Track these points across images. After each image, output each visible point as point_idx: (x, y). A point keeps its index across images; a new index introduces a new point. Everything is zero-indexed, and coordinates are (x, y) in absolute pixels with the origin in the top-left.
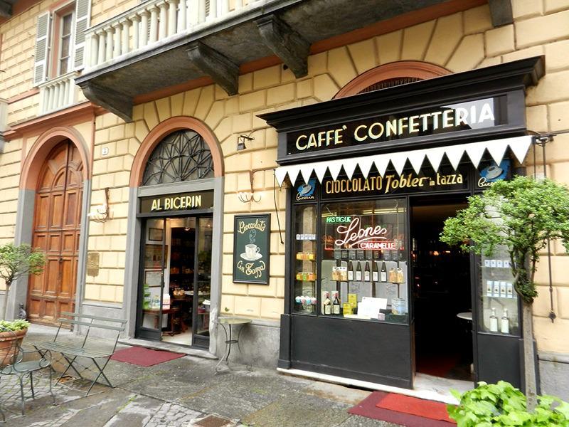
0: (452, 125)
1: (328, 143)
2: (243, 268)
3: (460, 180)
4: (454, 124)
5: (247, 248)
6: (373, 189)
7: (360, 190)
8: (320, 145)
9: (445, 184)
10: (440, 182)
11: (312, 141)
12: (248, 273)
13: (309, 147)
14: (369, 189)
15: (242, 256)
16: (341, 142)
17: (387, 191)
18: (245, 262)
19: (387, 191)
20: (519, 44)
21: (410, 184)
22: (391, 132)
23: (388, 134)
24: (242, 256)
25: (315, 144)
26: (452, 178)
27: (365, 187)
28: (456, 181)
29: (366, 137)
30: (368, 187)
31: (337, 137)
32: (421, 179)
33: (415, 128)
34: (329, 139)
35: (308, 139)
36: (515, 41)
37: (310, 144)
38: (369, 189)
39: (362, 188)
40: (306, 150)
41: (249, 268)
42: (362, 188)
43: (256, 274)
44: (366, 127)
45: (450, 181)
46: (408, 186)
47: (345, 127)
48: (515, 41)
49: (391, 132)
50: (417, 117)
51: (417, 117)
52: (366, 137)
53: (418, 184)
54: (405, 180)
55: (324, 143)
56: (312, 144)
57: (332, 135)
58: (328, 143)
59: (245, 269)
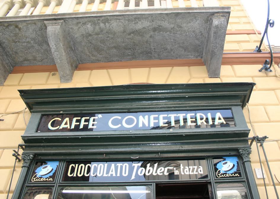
1: (81, 127)
3: (200, 171)
6: (118, 175)
7: (105, 175)
9: (188, 173)
10: (184, 172)
11: (66, 124)
13: (61, 128)
14: (114, 175)
17: (133, 177)
21: (156, 172)
22: (143, 124)
23: (140, 125)
26: (193, 169)
27: (110, 173)
28: (197, 171)
29: (120, 125)
32: (166, 169)
34: (83, 123)
37: (63, 126)
38: (114, 175)
39: (108, 173)
40: (55, 131)
42: (108, 173)
45: (193, 171)
46: (154, 174)
49: (143, 124)
50: (166, 115)
51: (166, 115)
52: (120, 125)
53: (163, 172)
54: (151, 168)
56: (66, 126)
58: (81, 127)
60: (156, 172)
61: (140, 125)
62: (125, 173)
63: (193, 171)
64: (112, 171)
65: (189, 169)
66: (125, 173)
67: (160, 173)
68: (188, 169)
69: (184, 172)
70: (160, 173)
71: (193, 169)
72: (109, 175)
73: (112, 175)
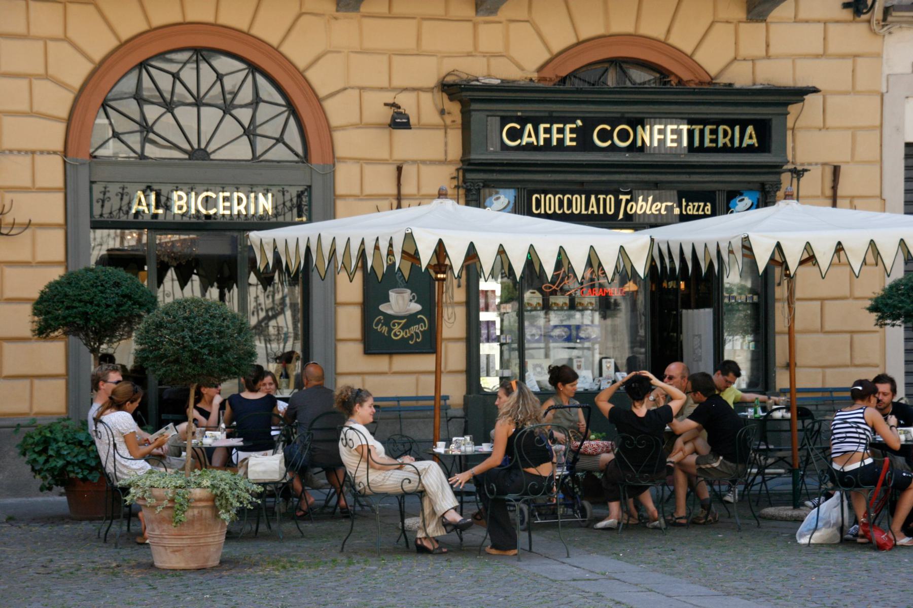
0: (714, 145)
1: (554, 143)
2: (385, 329)
4: (717, 145)
5: (392, 295)
6: (601, 212)
7: (584, 212)
8: (542, 143)
10: (686, 210)
12: (396, 335)
13: (524, 143)
14: (596, 212)
15: (383, 308)
16: (574, 144)
17: (621, 216)
18: (389, 319)
19: (621, 216)
20: (772, 51)
21: (651, 209)
24: (383, 308)
25: (533, 139)
26: (699, 207)
27: (591, 209)
28: (703, 210)
29: (609, 142)
30: (595, 209)
31: (568, 135)
33: (672, 141)
34: (555, 136)
35: (522, 131)
36: (768, 46)
37: (525, 140)
38: (596, 212)
39: (587, 208)
41: (396, 328)
43: (411, 338)
44: (609, 128)
45: (698, 210)
47: (579, 123)
48: (768, 46)
52: (609, 142)
55: (548, 141)
57: (561, 131)
58: (554, 143)
59: (390, 330)
60: (651, 209)
61: (639, 143)
62: (610, 210)
63: (698, 210)
64: (593, 207)
65: (694, 206)
66: (610, 210)
67: (656, 211)
68: (691, 207)
69: (686, 210)
70: (656, 211)
71: (699, 207)
72: (590, 212)
73: (593, 212)
